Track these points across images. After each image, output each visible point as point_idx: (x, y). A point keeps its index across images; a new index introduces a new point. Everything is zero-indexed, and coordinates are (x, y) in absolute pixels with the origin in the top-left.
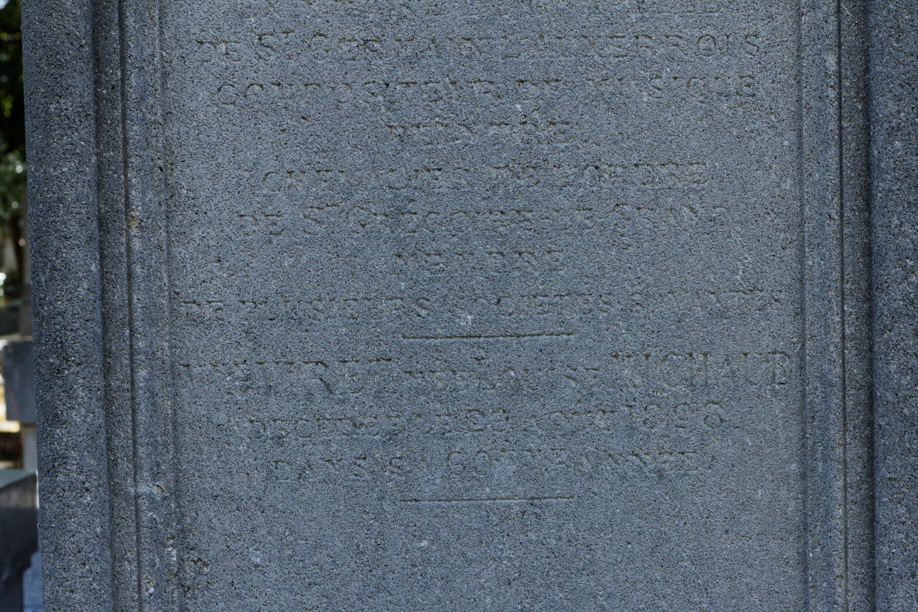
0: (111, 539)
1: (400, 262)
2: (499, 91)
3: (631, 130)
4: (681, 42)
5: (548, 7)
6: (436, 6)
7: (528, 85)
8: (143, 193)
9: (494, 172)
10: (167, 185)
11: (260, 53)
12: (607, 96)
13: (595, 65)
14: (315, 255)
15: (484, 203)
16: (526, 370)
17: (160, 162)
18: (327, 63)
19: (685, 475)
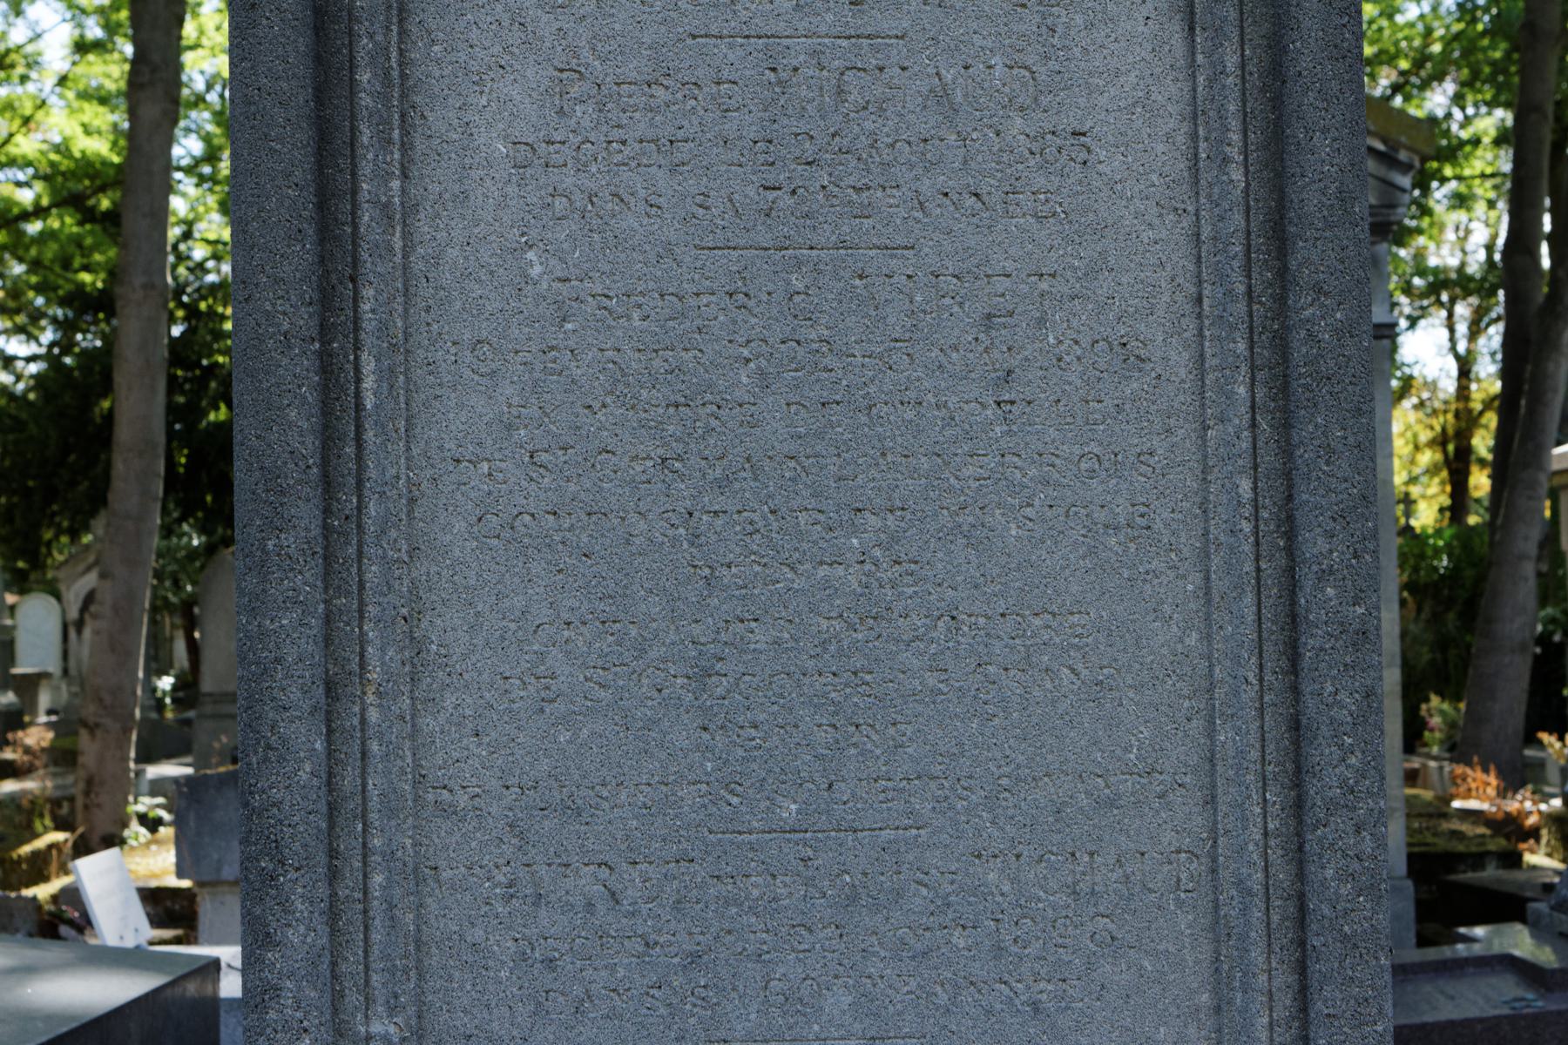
1: (706, 736)
2: (831, 522)
3: (996, 571)
4: (1058, 462)
5: (892, 418)
6: (752, 416)
7: (867, 514)
8: (383, 650)
9: (824, 624)
10: (412, 638)
11: (531, 474)
12: (965, 528)
13: (950, 489)
14: (599, 729)
15: (811, 663)
16: (865, 874)
17: (404, 611)
18: (616, 486)
19: (1067, 1008)
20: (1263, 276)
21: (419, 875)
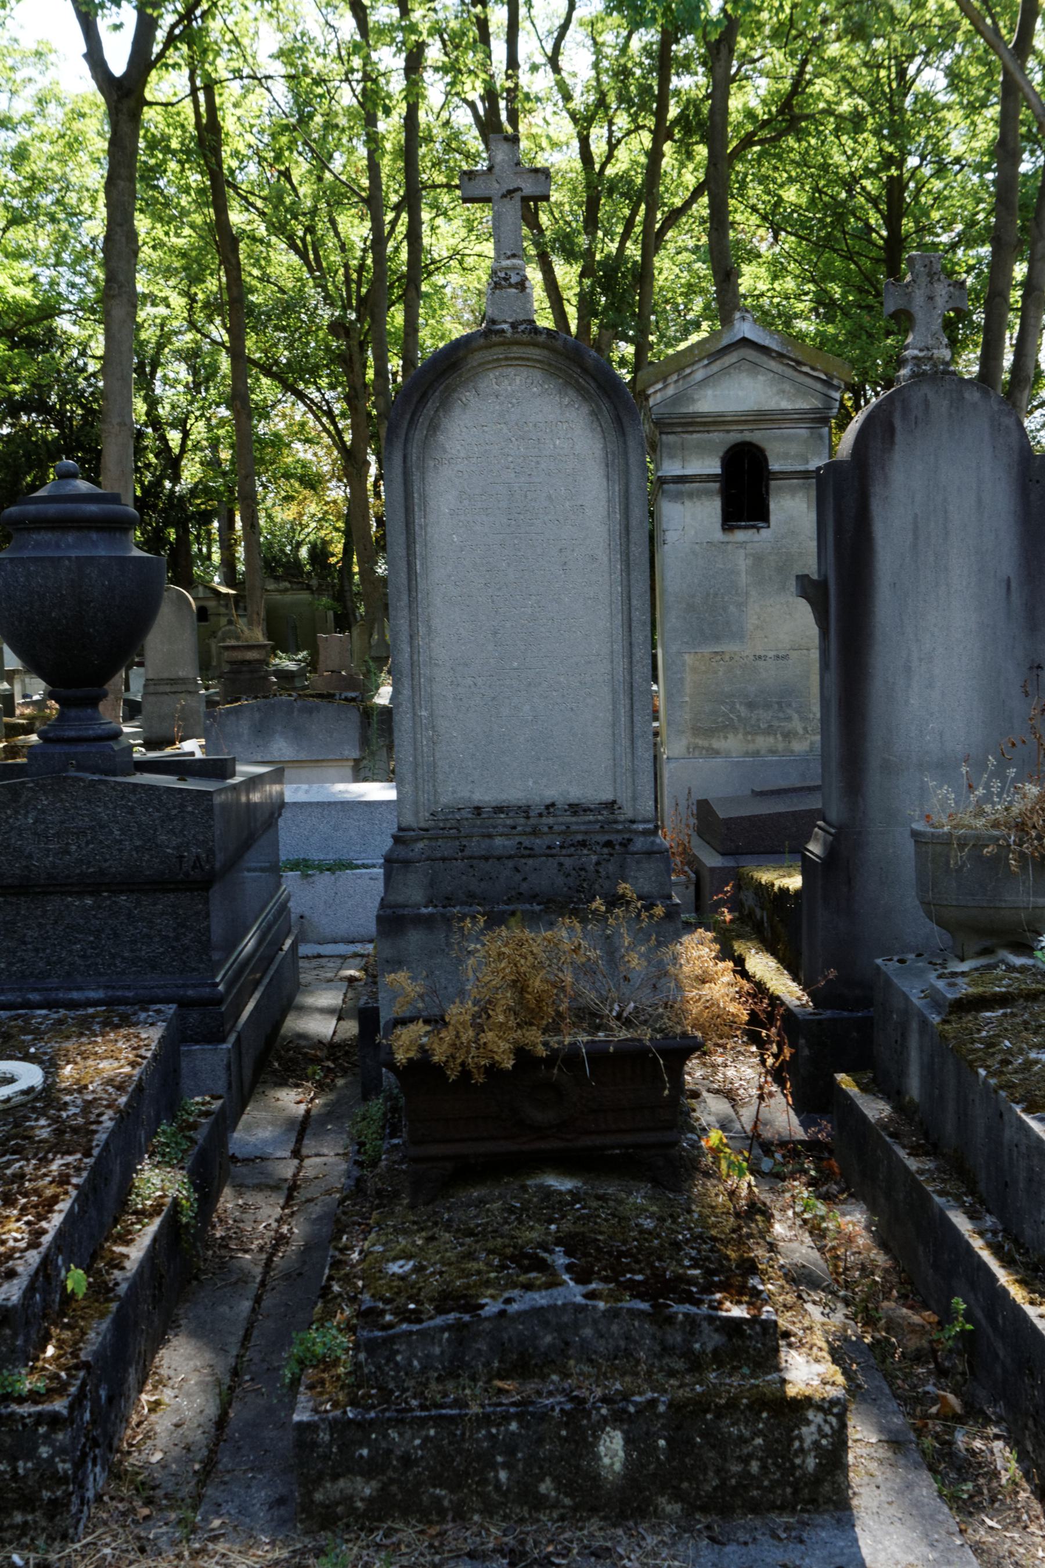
0: (414, 727)
20: (624, 540)
21: (431, 680)
